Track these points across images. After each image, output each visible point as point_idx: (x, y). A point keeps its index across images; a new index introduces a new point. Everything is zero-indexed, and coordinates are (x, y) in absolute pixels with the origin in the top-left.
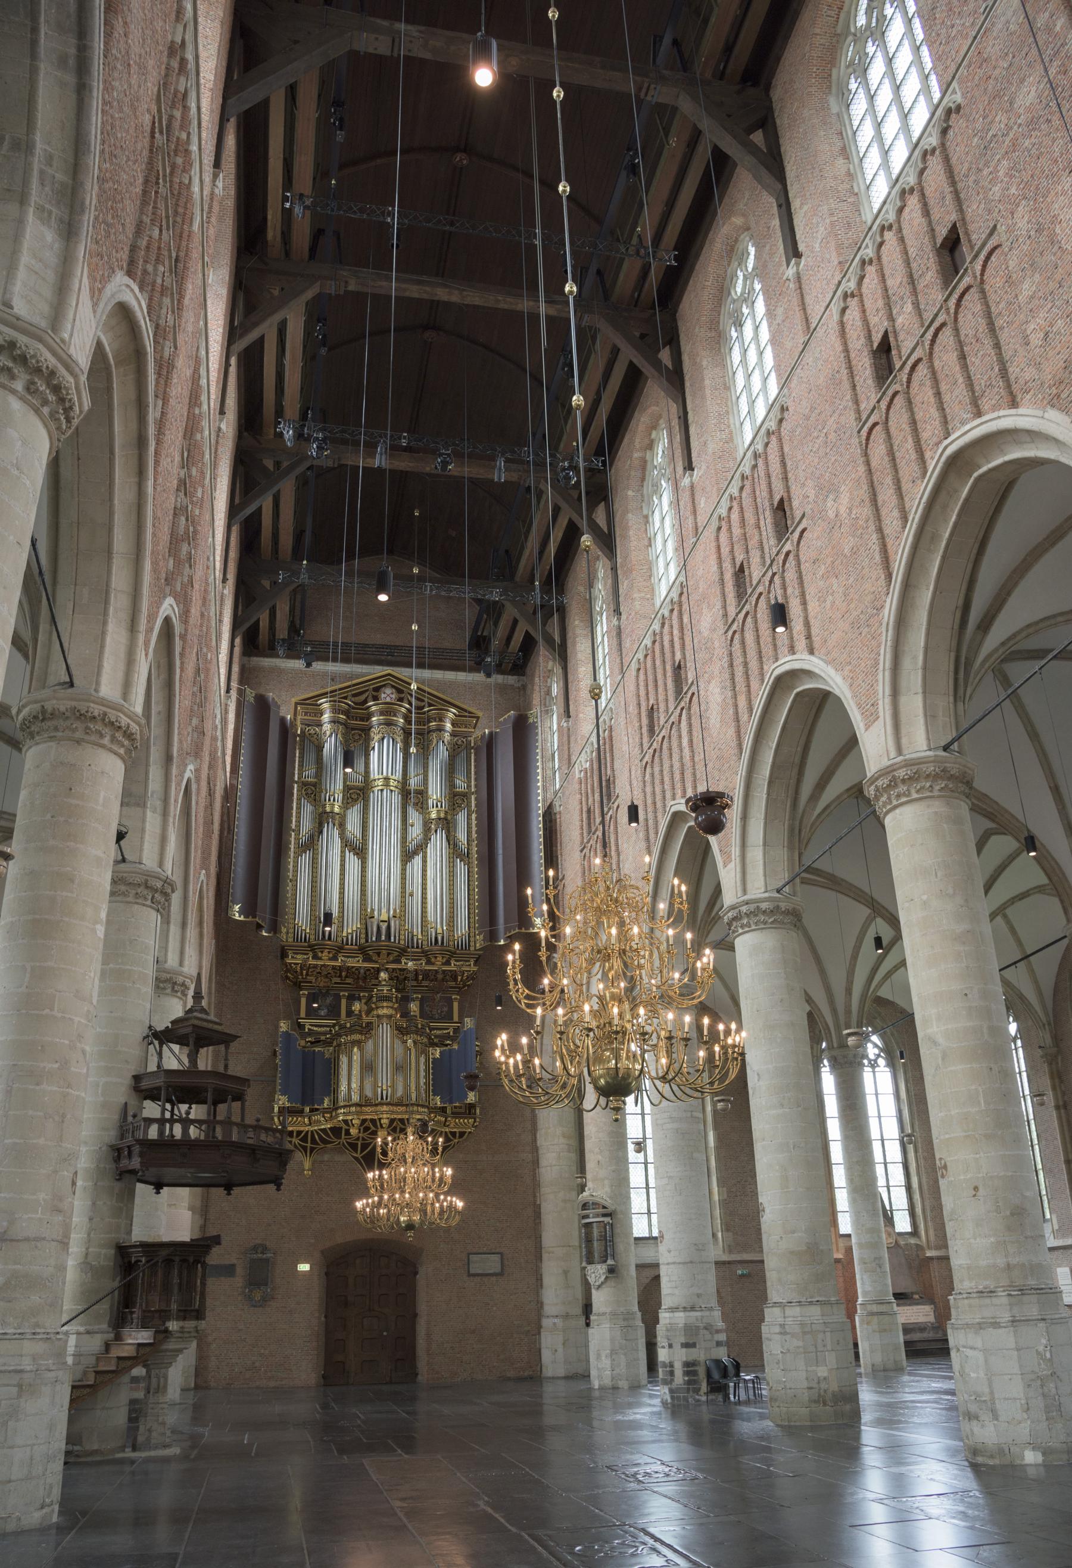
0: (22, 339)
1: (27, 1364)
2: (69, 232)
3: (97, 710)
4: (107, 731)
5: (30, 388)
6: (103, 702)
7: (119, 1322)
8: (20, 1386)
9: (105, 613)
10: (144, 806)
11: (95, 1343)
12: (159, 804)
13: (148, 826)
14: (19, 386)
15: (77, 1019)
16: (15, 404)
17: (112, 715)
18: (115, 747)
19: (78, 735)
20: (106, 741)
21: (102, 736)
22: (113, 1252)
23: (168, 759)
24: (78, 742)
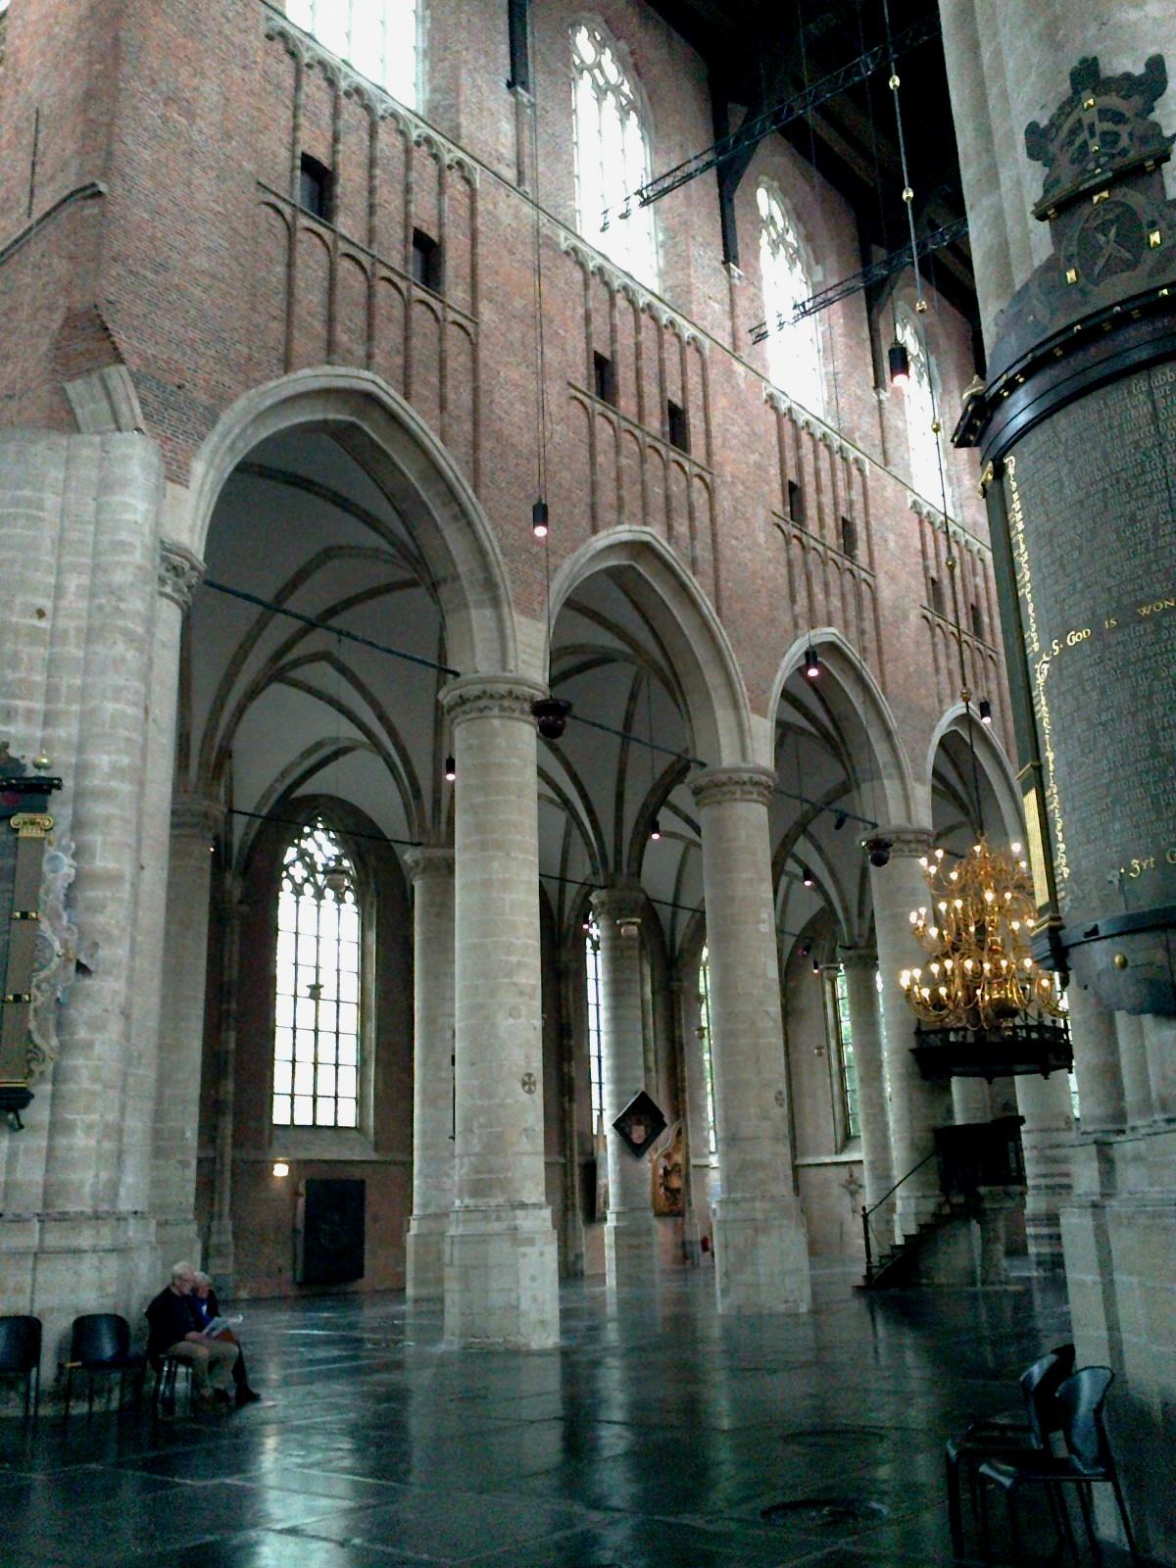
0: (489, 688)
1: (759, 1216)
2: (496, 603)
3: (724, 778)
4: (738, 790)
5: (502, 709)
6: (725, 771)
7: (945, 1188)
8: (756, 1230)
9: (712, 708)
10: (880, 778)
11: (930, 1206)
12: (893, 771)
13: (889, 792)
14: (496, 711)
15: (755, 992)
16: (496, 722)
17: (736, 777)
18: (749, 797)
19: (719, 797)
20: (738, 796)
21: (734, 793)
22: (930, 1135)
23: (888, 734)
24: (719, 803)
